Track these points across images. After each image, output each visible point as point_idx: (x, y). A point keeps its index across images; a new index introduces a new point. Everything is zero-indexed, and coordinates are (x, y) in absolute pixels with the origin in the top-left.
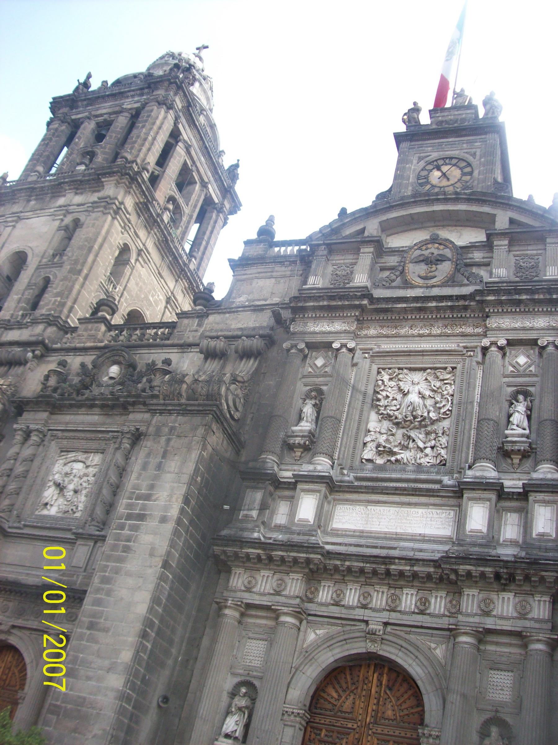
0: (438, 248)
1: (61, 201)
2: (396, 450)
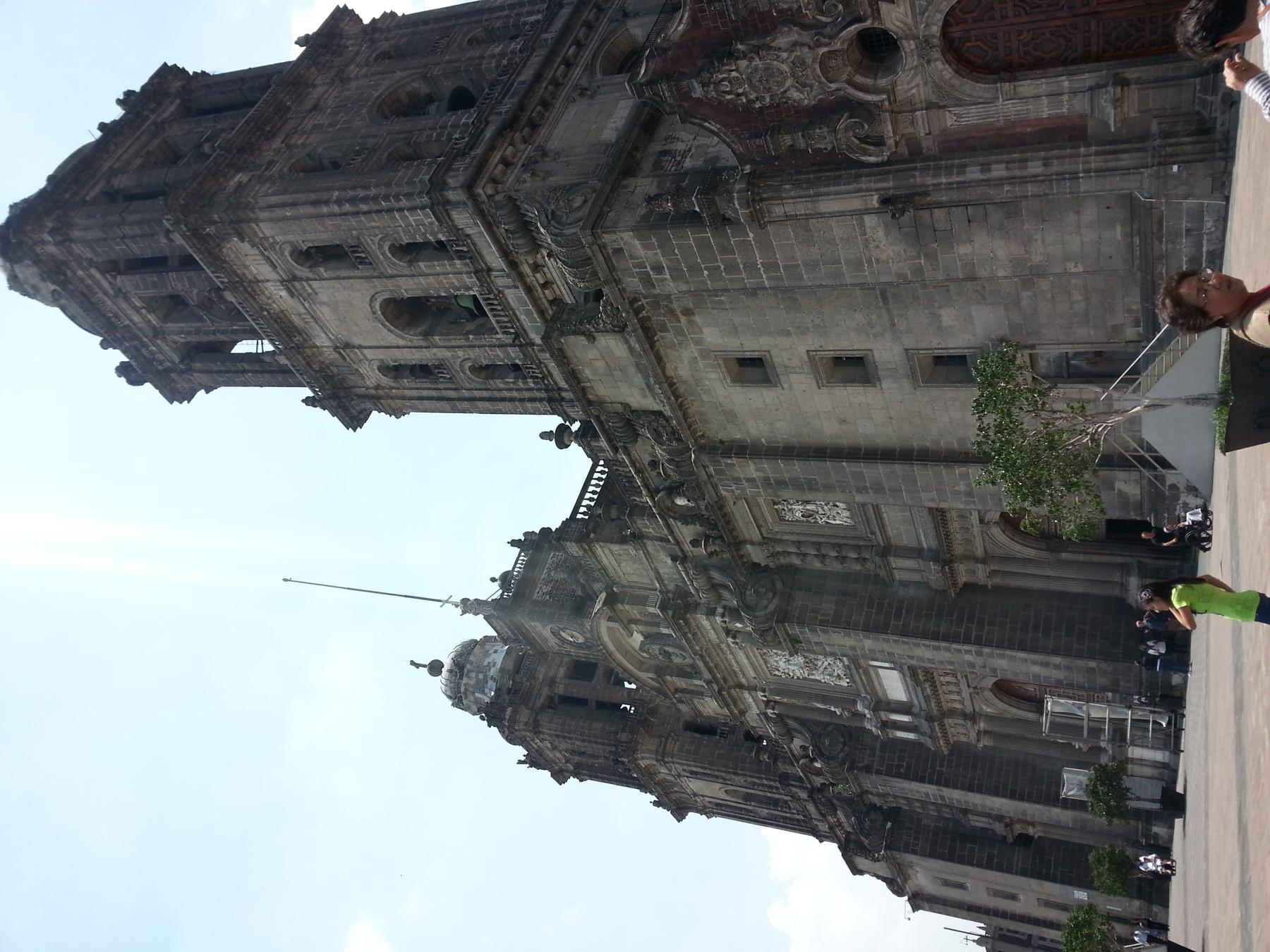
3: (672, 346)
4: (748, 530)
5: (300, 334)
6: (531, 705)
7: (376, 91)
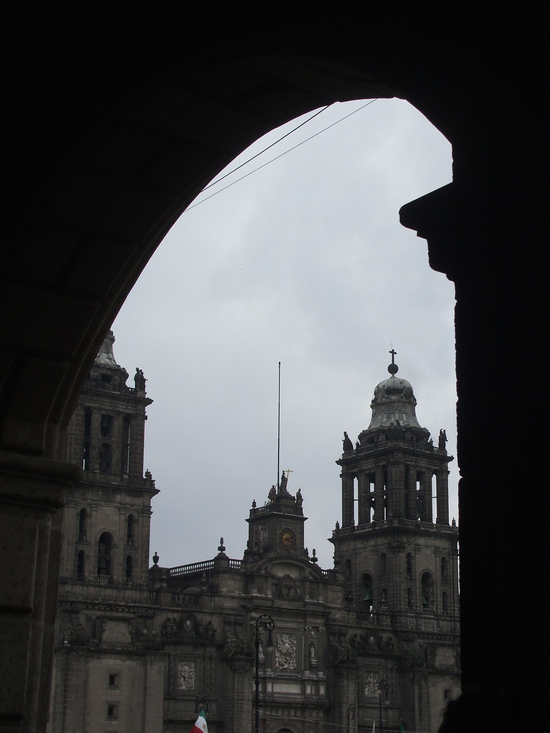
0: (290, 582)
1: (118, 498)
2: (284, 664)
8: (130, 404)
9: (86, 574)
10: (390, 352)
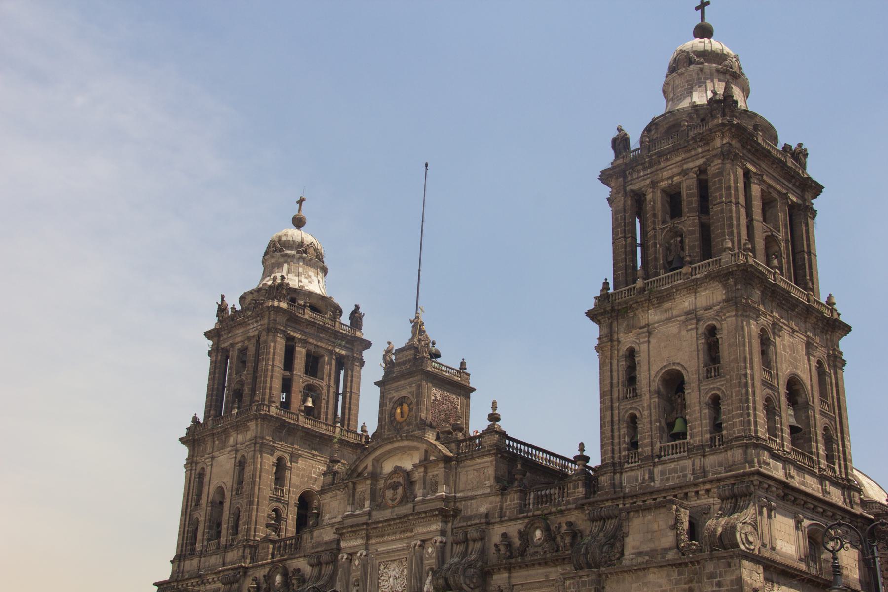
1: (232, 440)
3: (668, 575)
4: (520, 576)
5: (658, 304)
6: (288, 323)
7: (801, 372)
8: (259, 323)
9: (197, 545)
10: (697, 9)
